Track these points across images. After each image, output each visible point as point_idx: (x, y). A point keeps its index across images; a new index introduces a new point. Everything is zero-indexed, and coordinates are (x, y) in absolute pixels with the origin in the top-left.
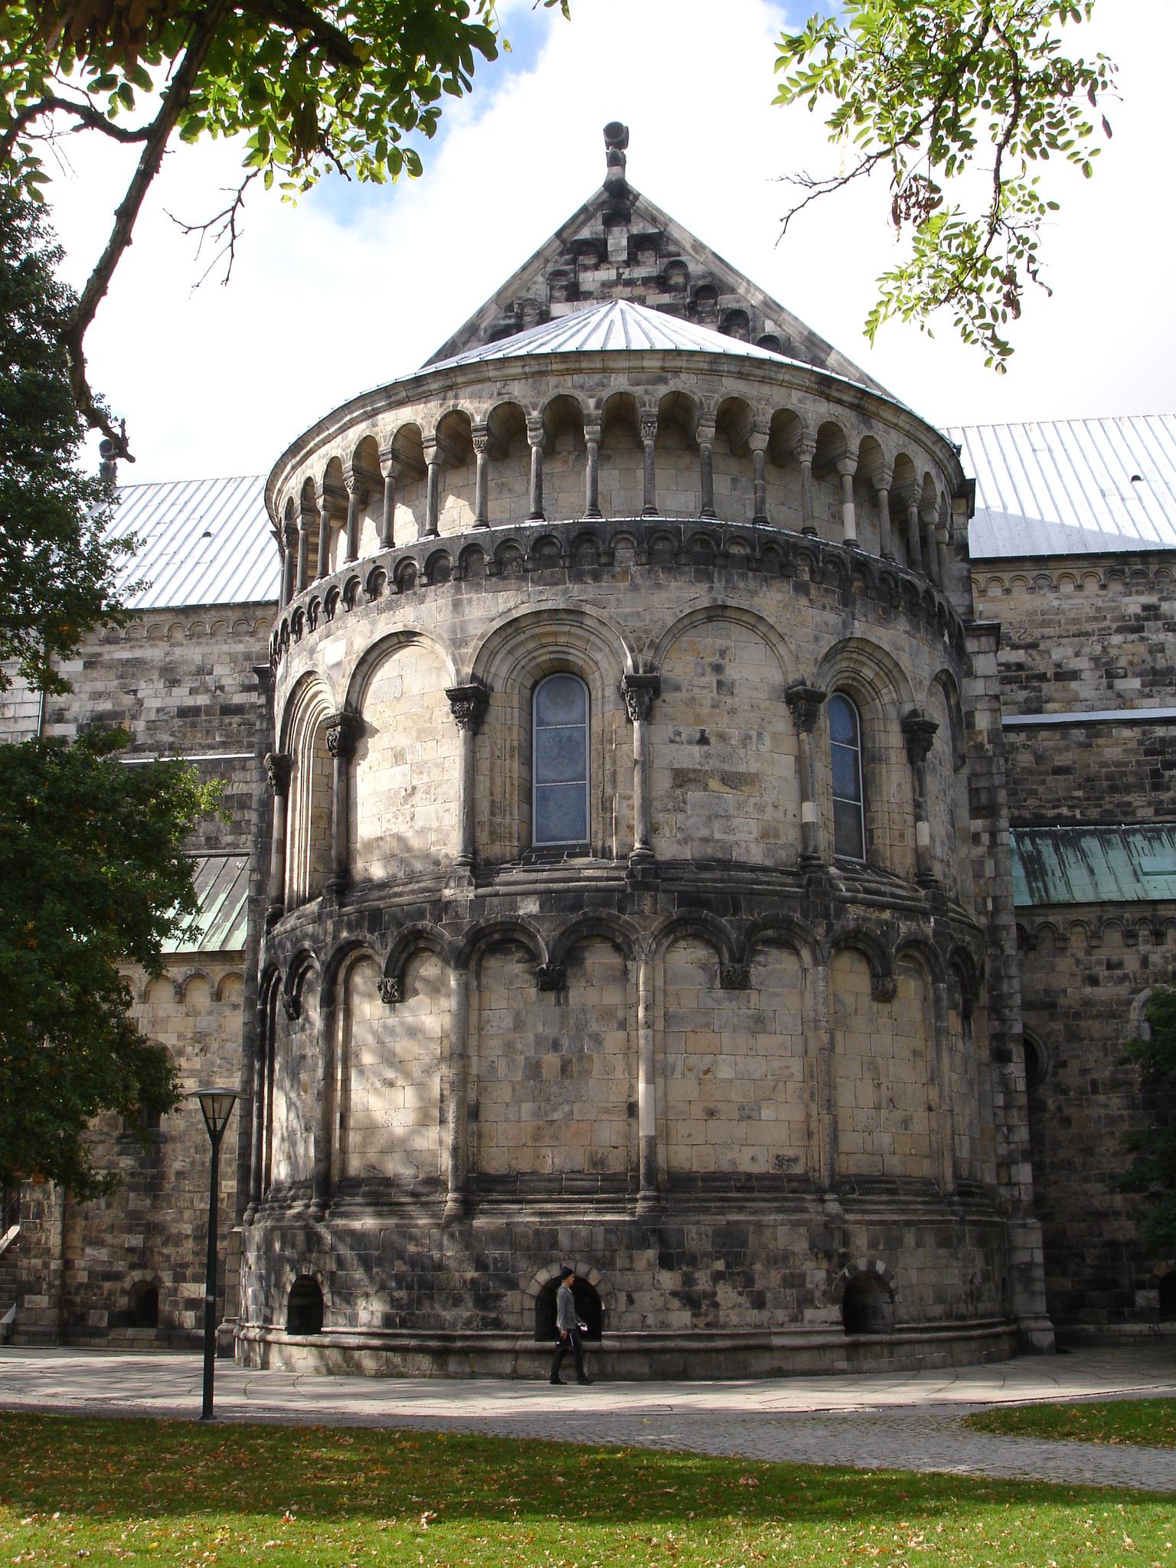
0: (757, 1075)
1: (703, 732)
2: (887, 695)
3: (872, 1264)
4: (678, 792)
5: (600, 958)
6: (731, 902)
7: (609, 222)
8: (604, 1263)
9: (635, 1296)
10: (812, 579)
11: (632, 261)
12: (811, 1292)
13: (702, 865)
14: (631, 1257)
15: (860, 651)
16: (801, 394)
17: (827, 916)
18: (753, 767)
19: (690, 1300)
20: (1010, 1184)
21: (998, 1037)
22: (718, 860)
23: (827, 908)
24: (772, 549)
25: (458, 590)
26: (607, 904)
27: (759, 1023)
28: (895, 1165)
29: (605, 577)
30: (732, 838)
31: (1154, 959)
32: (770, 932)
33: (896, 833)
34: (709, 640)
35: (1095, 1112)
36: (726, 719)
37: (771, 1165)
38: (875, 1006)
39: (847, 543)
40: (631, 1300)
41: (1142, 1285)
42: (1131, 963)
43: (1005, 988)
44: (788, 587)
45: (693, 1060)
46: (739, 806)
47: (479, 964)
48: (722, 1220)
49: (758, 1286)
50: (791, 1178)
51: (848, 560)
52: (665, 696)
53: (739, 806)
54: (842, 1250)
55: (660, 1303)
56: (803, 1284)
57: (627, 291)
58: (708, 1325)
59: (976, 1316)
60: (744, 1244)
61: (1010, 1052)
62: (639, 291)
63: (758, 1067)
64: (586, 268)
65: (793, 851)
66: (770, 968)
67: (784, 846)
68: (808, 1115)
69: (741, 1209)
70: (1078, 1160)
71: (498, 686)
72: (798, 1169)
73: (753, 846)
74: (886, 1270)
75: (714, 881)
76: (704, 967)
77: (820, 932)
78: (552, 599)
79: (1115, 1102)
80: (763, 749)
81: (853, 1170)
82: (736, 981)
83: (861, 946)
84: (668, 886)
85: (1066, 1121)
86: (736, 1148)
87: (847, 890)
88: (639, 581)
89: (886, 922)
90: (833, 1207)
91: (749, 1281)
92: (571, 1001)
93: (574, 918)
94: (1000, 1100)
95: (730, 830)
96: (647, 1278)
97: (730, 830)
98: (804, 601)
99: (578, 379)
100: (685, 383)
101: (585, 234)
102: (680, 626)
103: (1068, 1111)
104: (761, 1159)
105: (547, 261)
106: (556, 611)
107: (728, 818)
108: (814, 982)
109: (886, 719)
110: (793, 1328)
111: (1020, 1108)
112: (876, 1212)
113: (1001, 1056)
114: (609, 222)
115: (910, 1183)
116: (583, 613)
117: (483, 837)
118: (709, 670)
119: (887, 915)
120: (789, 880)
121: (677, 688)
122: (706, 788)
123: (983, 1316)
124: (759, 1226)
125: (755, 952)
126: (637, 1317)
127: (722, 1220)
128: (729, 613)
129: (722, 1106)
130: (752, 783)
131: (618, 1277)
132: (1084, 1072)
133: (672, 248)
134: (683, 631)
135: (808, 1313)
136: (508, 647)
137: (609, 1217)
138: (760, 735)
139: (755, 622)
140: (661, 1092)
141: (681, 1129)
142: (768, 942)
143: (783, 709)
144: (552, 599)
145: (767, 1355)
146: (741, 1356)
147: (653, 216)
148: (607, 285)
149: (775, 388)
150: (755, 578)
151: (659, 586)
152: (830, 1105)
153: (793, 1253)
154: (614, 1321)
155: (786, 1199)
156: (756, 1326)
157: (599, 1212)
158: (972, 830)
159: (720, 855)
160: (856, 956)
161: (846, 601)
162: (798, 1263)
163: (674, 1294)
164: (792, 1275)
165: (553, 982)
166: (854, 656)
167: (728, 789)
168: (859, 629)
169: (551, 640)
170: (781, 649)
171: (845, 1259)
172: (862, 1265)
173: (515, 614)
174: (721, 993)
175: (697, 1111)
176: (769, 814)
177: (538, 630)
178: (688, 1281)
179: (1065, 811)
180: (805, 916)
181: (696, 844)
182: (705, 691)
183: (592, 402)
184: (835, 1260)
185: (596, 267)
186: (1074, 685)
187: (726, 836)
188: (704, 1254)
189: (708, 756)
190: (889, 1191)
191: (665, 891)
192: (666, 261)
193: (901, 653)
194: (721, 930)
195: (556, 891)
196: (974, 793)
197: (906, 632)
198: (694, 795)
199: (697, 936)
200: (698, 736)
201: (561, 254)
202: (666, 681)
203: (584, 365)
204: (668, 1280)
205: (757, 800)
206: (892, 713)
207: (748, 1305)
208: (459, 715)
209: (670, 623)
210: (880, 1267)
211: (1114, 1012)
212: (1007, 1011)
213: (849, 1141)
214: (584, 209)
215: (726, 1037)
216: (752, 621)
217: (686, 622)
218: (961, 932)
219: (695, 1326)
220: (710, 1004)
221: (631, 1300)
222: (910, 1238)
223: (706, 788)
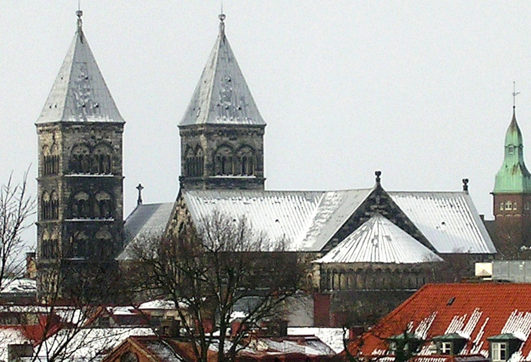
11: (380, 204)
57: (379, 211)
101: (372, 197)
148: (375, 209)
185: (374, 204)
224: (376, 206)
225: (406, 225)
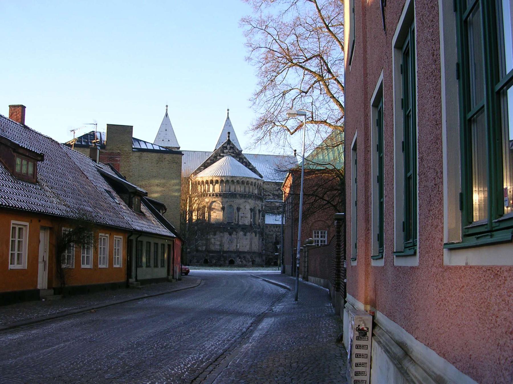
2: (257, 208)
8: (235, 258)
13: (243, 225)
19: (242, 262)
20: (263, 252)
21: (263, 239)
27: (247, 239)
31: (276, 230)
42: (274, 230)
57: (229, 153)
62: (231, 153)
79: (271, 244)
82: (245, 235)
94: (262, 244)
100: (244, 179)
101: (225, 145)
114: (228, 144)
132: (268, 241)
143: (250, 211)
147: (233, 145)
148: (227, 152)
152: (252, 246)
161: (255, 200)
171: (252, 259)
176: (248, 220)
178: (241, 260)
186: (270, 197)
196: (262, 215)
198: (243, 219)
211: (272, 235)
224: (227, 151)
225: (245, 161)
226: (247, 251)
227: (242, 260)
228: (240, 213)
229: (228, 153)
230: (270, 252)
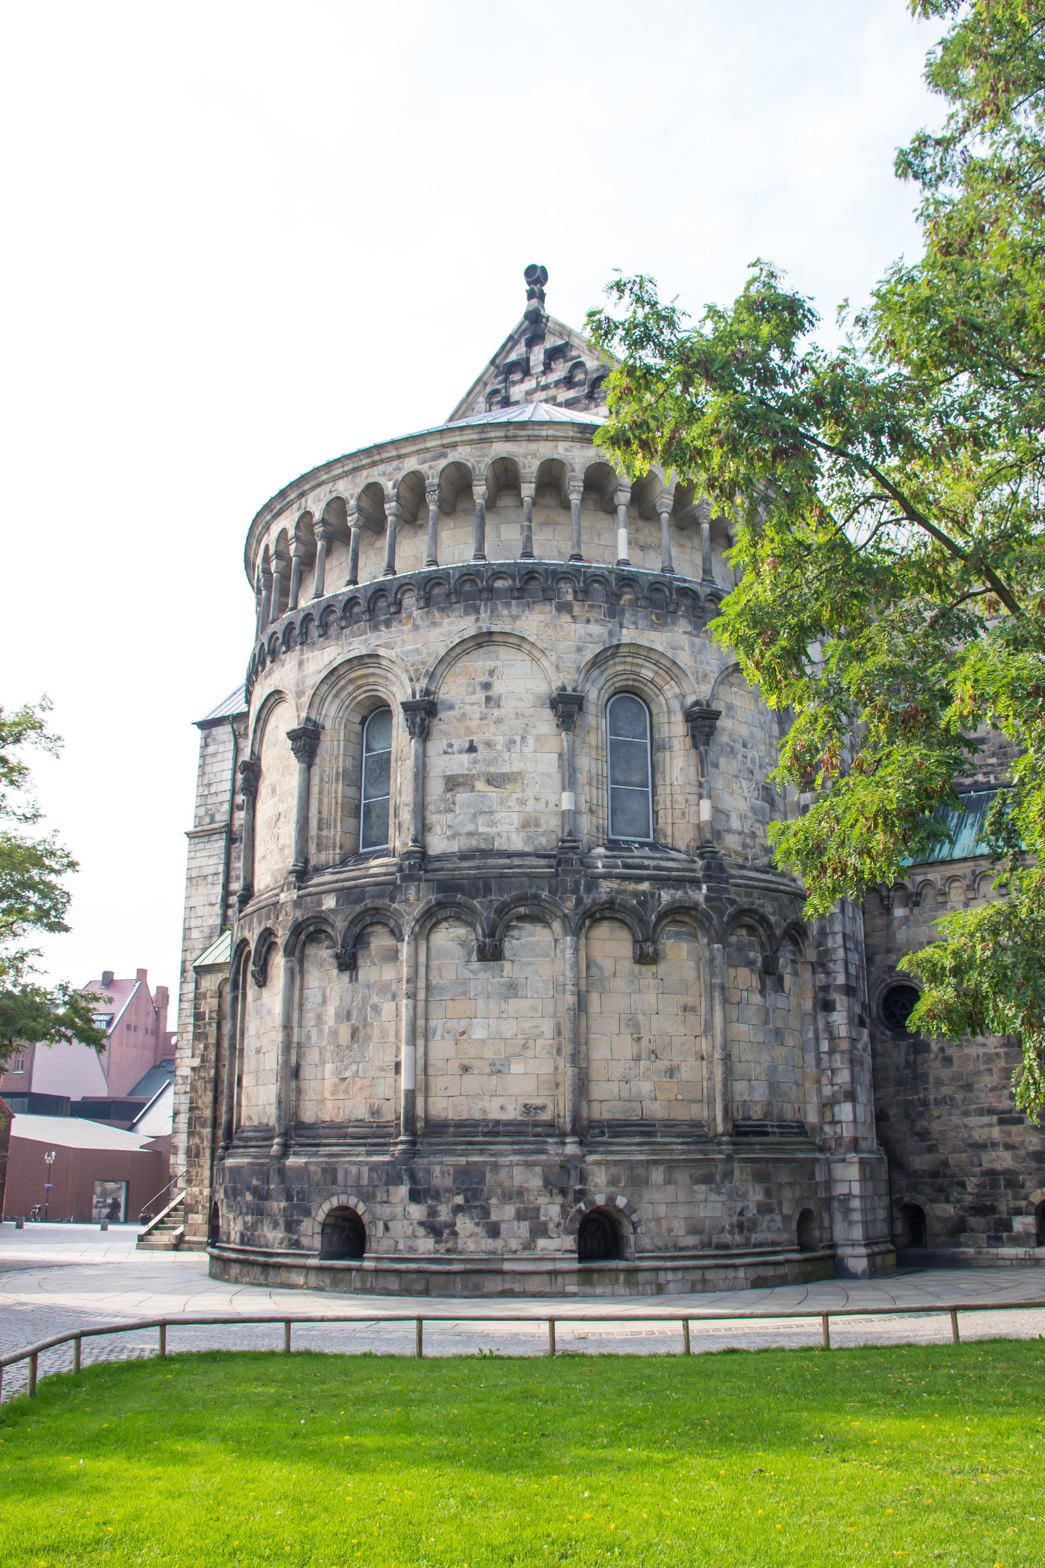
0: (508, 1035)
1: (472, 742)
2: (671, 690)
3: (611, 1199)
4: (449, 795)
5: (380, 940)
6: (482, 886)
7: (530, 344)
8: (367, 1197)
9: (391, 1224)
10: (575, 599)
11: (548, 368)
12: (545, 1224)
13: (464, 856)
14: (388, 1191)
15: (635, 655)
16: (567, 444)
17: (576, 891)
18: (515, 769)
19: (434, 1229)
22: (482, 851)
23: (577, 884)
24: (534, 578)
25: (302, 652)
26: (382, 895)
27: (512, 989)
28: (657, 1110)
29: (394, 624)
30: (495, 830)
32: (522, 910)
33: (678, 812)
34: (480, 663)
35: (972, 1051)
36: (493, 728)
37: (519, 1112)
38: (637, 968)
39: (619, 563)
40: (387, 1228)
41: (1018, 1212)
43: (830, 943)
44: (550, 609)
45: (451, 1024)
46: (502, 802)
47: (302, 951)
48: (463, 1160)
49: (494, 1217)
50: (536, 1124)
51: (612, 578)
52: (440, 715)
53: (502, 802)
54: (578, 1187)
55: (409, 1232)
56: (537, 1216)
58: (448, 1251)
59: (747, 1244)
60: (482, 1180)
61: (834, 1002)
63: (509, 1028)
64: (514, 383)
65: (554, 837)
66: (523, 941)
67: (544, 833)
68: (556, 1069)
69: (482, 1152)
70: (959, 1096)
71: (328, 725)
72: (546, 1116)
73: (514, 837)
74: (627, 1205)
75: (470, 868)
76: (463, 944)
77: (570, 904)
78: (357, 646)
80: (526, 750)
81: (607, 1116)
83: (618, 916)
84: (429, 876)
85: (948, 1060)
86: (487, 1098)
87: (604, 867)
88: (419, 622)
89: (644, 893)
90: (571, 1148)
91: (486, 1212)
92: (360, 978)
93: (358, 908)
95: (493, 824)
96: (399, 1210)
97: (493, 824)
98: (566, 618)
99: (381, 468)
100: (462, 454)
101: (513, 357)
102: (453, 654)
103: (949, 1052)
104: (510, 1107)
105: (486, 384)
106: (361, 657)
107: (491, 813)
108: (563, 951)
109: (669, 711)
110: (526, 1254)
111: (842, 1052)
112: (623, 1152)
113: (828, 1006)
115: (673, 1126)
116: (378, 656)
117: (313, 848)
118: (478, 688)
119: (645, 886)
120: (543, 862)
121: (451, 707)
122: (473, 789)
123: (756, 1246)
124: (496, 1166)
125: (509, 927)
126: (391, 1242)
127: (463, 1160)
128: (495, 638)
129: (475, 1063)
130: (515, 781)
131: (378, 1209)
133: (574, 353)
134: (458, 657)
135: (541, 1243)
136: (334, 692)
137: (375, 1158)
138: (523, 738)
139: (518, 642)
140: (421, 1051)
141: (438, 1084)
142: (521, 918)
143: (548, 714)
144: (357, 646)
145: (499, 1278)
146: (474, 1278)
148: (529, 393)
149: (542, 444)
150: (518, 605)
151: (434, 624)
153: (528, 1190)
154: (374, 1246)
155: (527, 1143)
156: (490, 1253)
157: (369, 1154)
158: (802, 803)
159: (483, 846)
160: (617, 925)
161: (614, 612)
162: (532, 1198)
163: (421, 1224)
164: (526, 1209)
165: (348, 963)
166: (629, 659)
167: (492, 788)
168: (627, 635)
169: (364, 681)
170: (545, 663)
171: (580, 1195)
172: (600, 1200)
173: (335, 665)
174: (476, 965)
175: (454, 1067)
176: (531, 806)
177: (353, 675)
178: (433, 1213)
179: (980, 778)
180: (553, 892)
181: (463, 838)
182: (475, 707)
183: (390, 484)
184: (571, 1196)
185: (522, 381)
187: (489, 829)
188: (447, 1190)
189: (475, 761)
190: (643, 1134)
191: (427, 881)
192: (570, 364)
193: (680, 653)
194: (473, 911)
195: (348, 888)
197: (685, 633)
198: (462, 797)
199: (458, 918)
200: (467, 745)
201: (496, 376)
202: (442, 703)
203: (384, 456)
204: (417, 1212)
205: (519, 795)
206: (676, 705)
207: (484, 1234)
208: (295, 750)
209: (442, 652)
210: (621, 1202)
212: (831, 965)
213: (600, 1090)
214: (511, 338)
215: (481, 1002)
216: (517, 641)
217: (458, 650)
218: (750, 895)
219: (437, 1251)
220: (468, 975)
221: (387, 1228)
222: (657, 1175)
223: (473, 789)
226: (512, 1113)
227: (444, 1213)
228: (436, 746)
229: (542, 395)
230: (991, 1111)
